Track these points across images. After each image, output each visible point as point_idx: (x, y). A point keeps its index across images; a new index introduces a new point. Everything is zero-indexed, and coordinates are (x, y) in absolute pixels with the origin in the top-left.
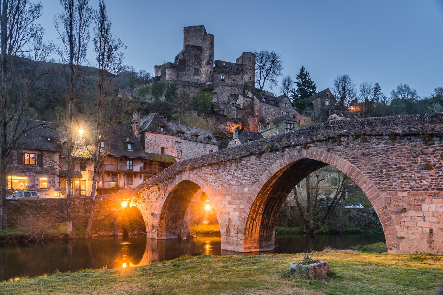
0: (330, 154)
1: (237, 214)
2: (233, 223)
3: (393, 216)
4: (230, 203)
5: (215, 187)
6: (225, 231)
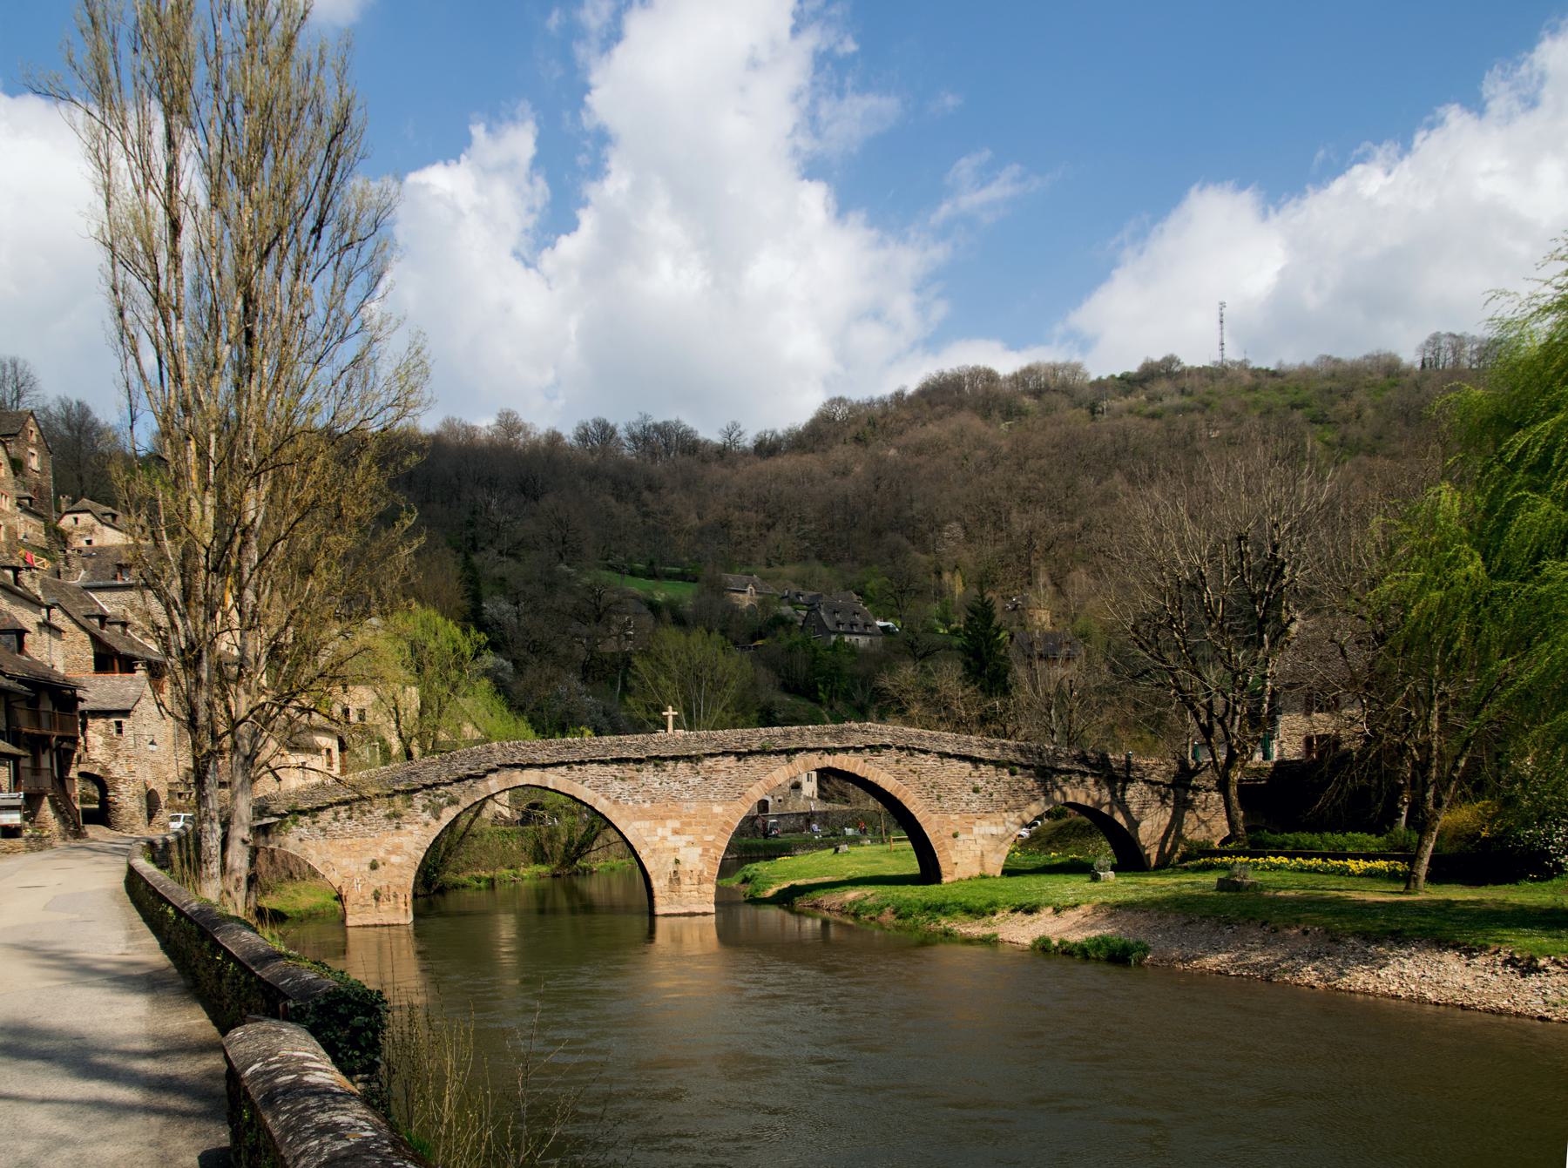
0: (868, 766)
1: (699, 850)
2: (688, 867)
3: (946, 841)
4: (676, 832)
5: (631, 803)
6: (667, 882)
